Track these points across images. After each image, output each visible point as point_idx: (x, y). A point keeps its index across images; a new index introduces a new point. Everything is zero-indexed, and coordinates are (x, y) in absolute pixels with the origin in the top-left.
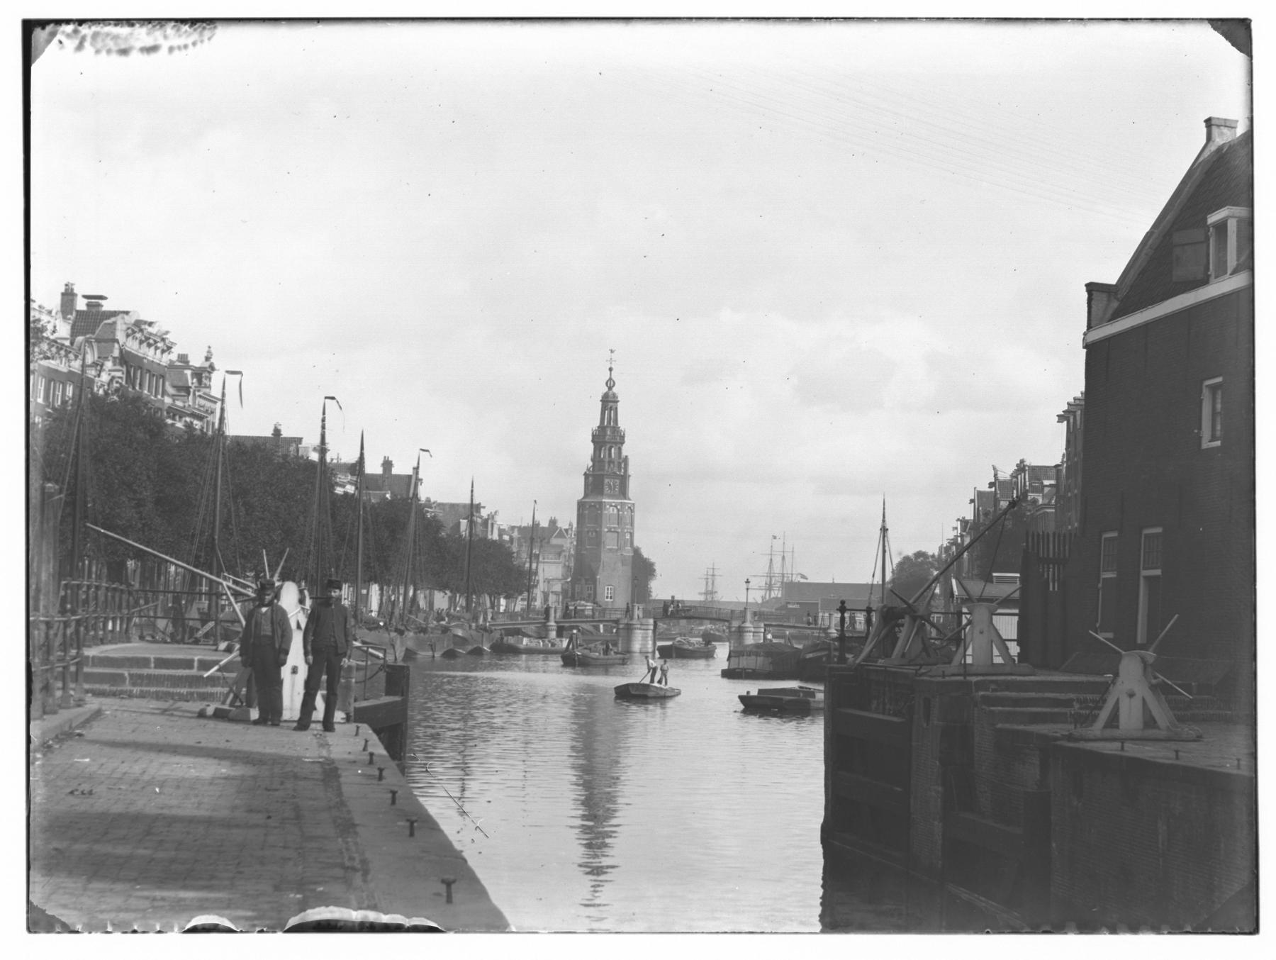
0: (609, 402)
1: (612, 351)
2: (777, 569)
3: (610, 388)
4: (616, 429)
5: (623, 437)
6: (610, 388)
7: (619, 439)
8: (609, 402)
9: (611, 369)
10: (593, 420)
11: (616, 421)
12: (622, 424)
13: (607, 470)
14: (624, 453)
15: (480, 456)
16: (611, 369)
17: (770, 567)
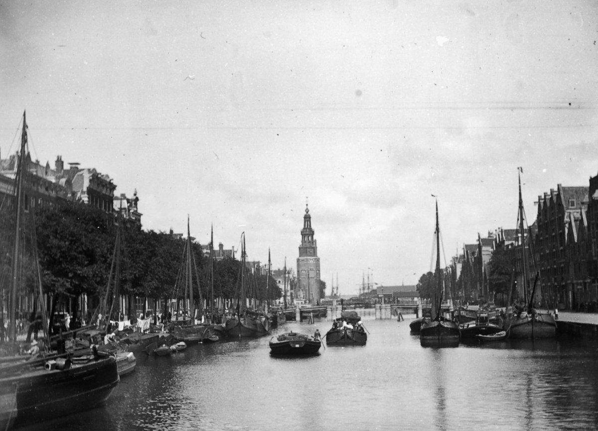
0: (307, 218)
1: (307, 197)
2: (366, 282)
3: (307, 212)
4: (310, 229)
5: (313, 232)
6: (307, 212)
7: (312, 233)
8: (307, 218)
9: (307, 205)
10: (301, 226)
11: (310, 226)
12: (313, 227)
13: (308, 246)
14: (314, 239)
15: (269, 247)
16: (307, 205)
17: (363, 281)
